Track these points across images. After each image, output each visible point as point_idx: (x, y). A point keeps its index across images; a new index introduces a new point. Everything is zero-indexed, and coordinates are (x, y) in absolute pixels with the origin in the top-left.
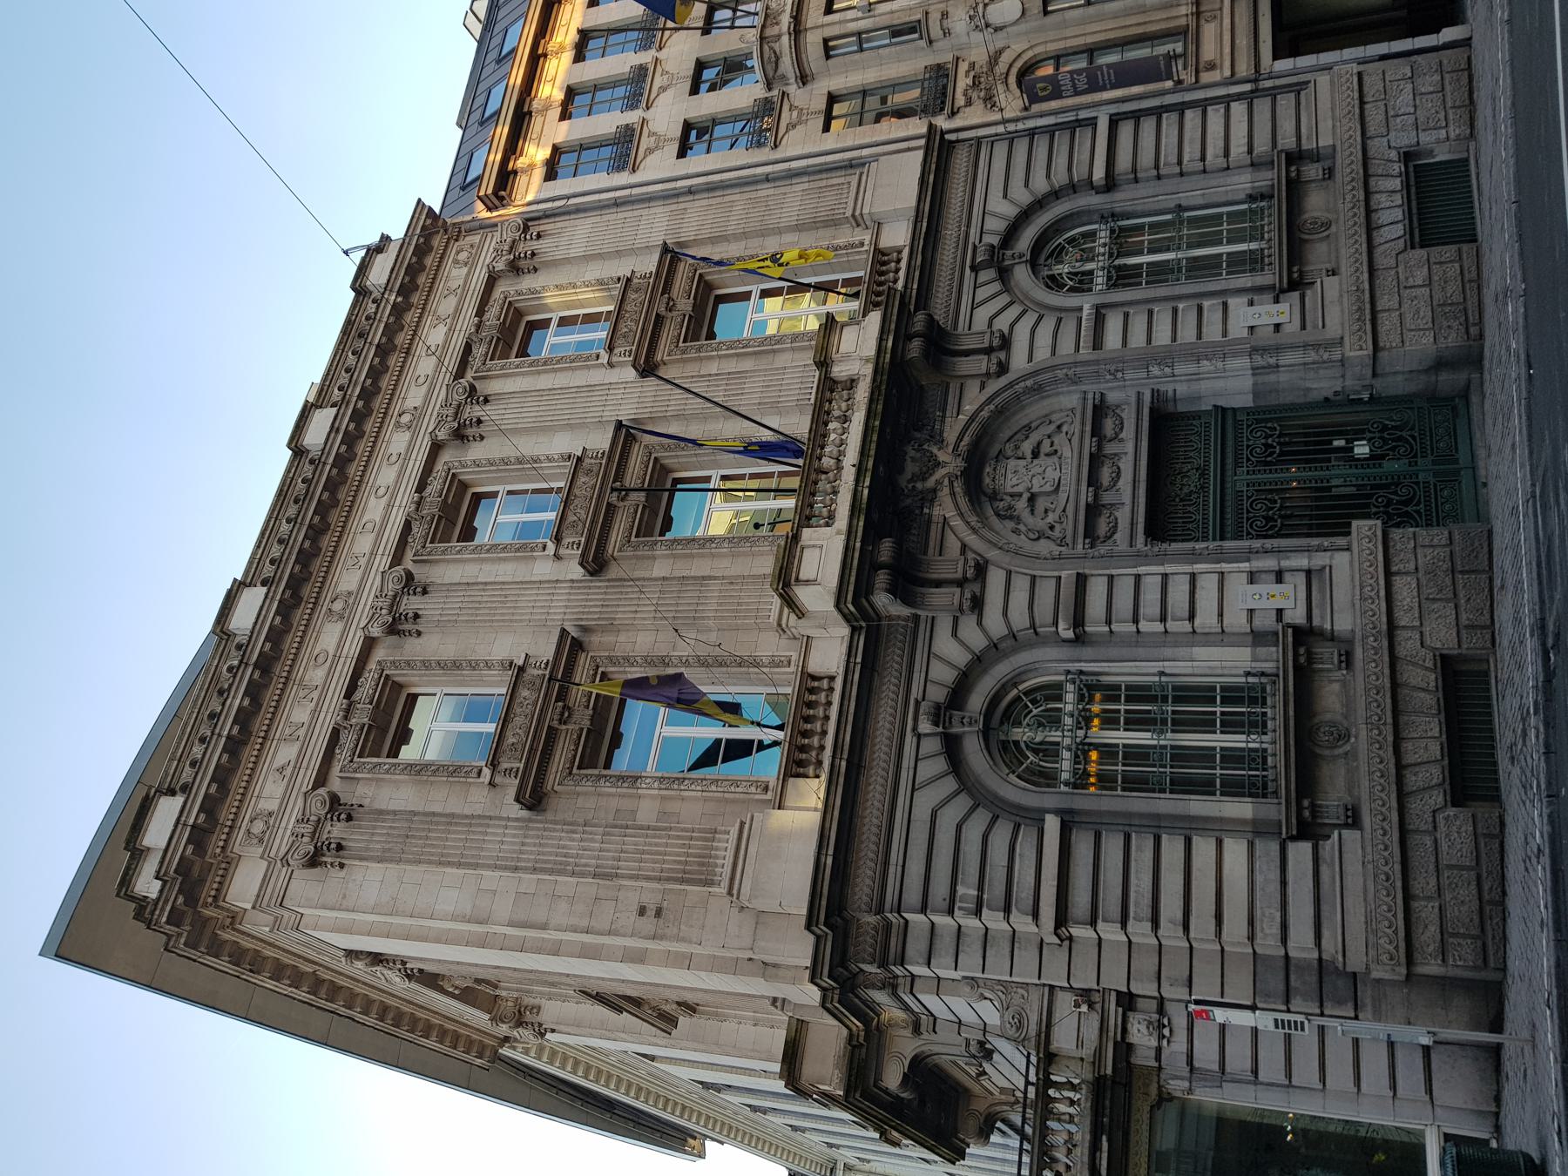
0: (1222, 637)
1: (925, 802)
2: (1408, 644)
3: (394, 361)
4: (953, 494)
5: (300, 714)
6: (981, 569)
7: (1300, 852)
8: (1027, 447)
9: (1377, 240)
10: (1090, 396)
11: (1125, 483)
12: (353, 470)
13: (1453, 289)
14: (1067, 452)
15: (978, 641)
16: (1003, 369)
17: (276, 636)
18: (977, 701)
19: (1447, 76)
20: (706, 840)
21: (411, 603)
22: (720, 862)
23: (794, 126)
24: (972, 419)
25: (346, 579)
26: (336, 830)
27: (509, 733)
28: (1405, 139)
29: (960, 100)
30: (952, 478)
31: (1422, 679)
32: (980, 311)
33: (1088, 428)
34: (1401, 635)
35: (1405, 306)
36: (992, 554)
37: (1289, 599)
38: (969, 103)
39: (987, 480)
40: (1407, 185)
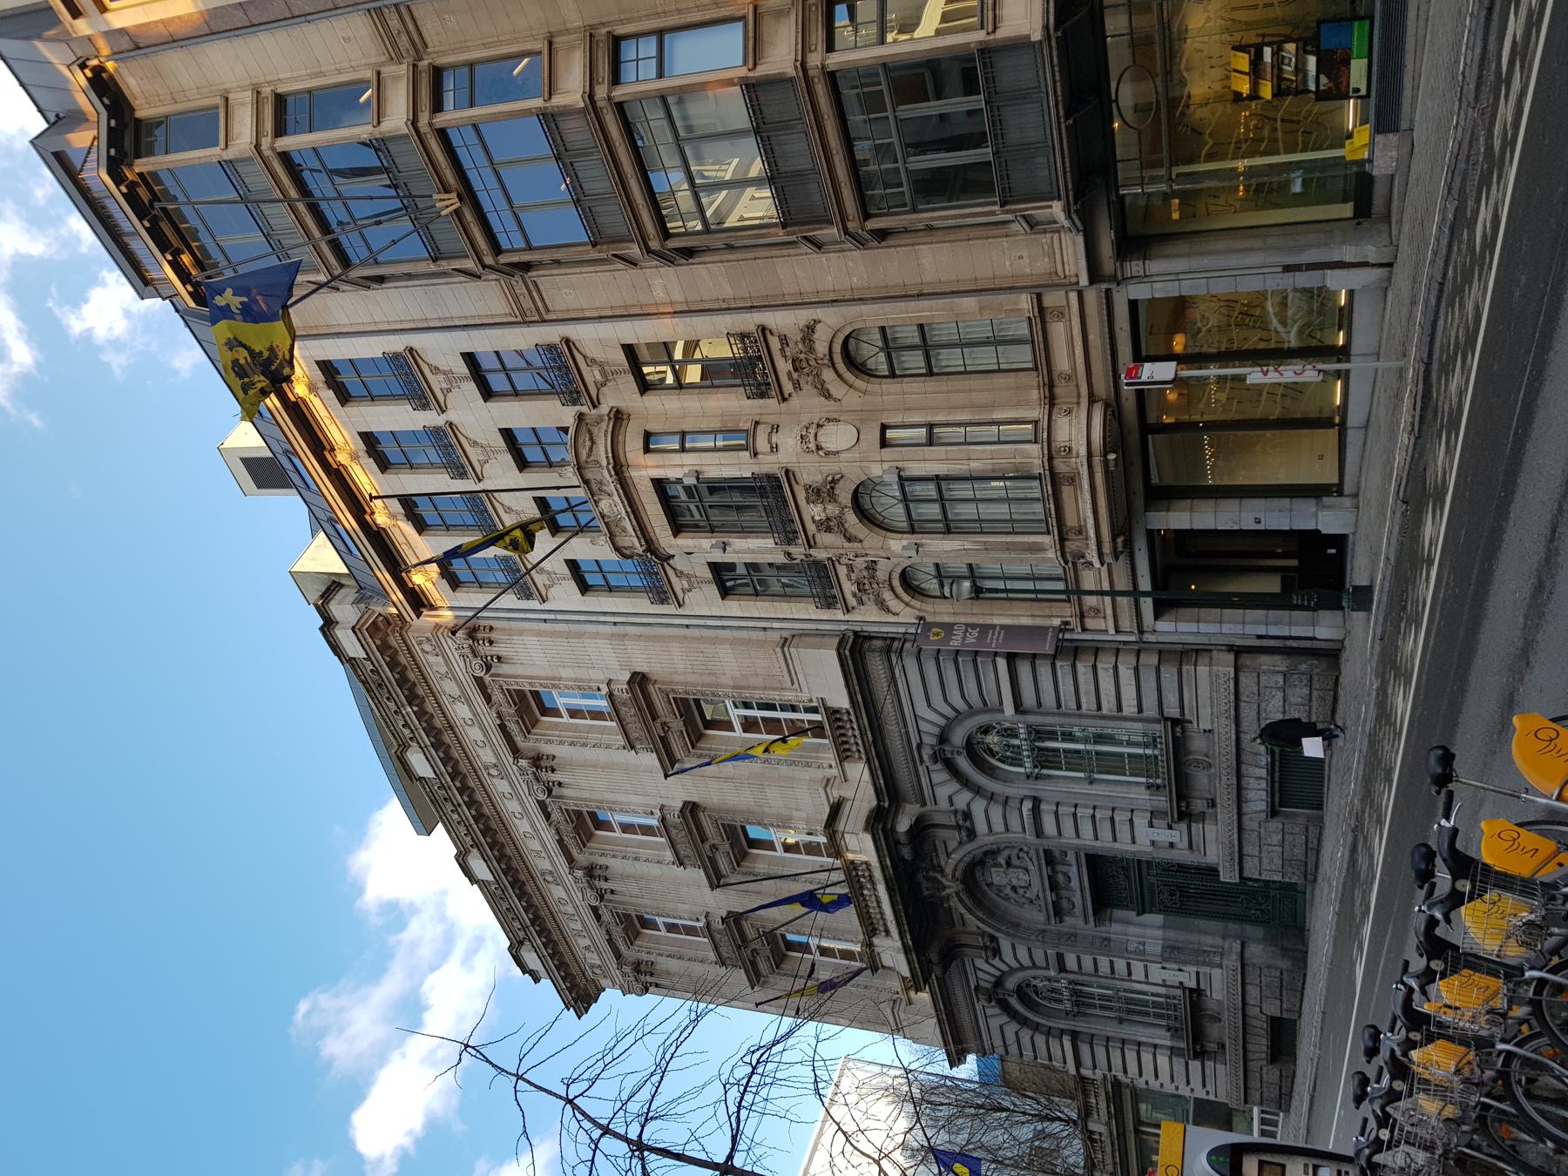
1: (994, 1023)
2: (1253, 1011)
8: (1001, 860)
11: (1075, 884)
13: (1299, 852)
14: (1031, 867)
16: (972, 834)
19: (1315, 694)
31: (1260, 1025)
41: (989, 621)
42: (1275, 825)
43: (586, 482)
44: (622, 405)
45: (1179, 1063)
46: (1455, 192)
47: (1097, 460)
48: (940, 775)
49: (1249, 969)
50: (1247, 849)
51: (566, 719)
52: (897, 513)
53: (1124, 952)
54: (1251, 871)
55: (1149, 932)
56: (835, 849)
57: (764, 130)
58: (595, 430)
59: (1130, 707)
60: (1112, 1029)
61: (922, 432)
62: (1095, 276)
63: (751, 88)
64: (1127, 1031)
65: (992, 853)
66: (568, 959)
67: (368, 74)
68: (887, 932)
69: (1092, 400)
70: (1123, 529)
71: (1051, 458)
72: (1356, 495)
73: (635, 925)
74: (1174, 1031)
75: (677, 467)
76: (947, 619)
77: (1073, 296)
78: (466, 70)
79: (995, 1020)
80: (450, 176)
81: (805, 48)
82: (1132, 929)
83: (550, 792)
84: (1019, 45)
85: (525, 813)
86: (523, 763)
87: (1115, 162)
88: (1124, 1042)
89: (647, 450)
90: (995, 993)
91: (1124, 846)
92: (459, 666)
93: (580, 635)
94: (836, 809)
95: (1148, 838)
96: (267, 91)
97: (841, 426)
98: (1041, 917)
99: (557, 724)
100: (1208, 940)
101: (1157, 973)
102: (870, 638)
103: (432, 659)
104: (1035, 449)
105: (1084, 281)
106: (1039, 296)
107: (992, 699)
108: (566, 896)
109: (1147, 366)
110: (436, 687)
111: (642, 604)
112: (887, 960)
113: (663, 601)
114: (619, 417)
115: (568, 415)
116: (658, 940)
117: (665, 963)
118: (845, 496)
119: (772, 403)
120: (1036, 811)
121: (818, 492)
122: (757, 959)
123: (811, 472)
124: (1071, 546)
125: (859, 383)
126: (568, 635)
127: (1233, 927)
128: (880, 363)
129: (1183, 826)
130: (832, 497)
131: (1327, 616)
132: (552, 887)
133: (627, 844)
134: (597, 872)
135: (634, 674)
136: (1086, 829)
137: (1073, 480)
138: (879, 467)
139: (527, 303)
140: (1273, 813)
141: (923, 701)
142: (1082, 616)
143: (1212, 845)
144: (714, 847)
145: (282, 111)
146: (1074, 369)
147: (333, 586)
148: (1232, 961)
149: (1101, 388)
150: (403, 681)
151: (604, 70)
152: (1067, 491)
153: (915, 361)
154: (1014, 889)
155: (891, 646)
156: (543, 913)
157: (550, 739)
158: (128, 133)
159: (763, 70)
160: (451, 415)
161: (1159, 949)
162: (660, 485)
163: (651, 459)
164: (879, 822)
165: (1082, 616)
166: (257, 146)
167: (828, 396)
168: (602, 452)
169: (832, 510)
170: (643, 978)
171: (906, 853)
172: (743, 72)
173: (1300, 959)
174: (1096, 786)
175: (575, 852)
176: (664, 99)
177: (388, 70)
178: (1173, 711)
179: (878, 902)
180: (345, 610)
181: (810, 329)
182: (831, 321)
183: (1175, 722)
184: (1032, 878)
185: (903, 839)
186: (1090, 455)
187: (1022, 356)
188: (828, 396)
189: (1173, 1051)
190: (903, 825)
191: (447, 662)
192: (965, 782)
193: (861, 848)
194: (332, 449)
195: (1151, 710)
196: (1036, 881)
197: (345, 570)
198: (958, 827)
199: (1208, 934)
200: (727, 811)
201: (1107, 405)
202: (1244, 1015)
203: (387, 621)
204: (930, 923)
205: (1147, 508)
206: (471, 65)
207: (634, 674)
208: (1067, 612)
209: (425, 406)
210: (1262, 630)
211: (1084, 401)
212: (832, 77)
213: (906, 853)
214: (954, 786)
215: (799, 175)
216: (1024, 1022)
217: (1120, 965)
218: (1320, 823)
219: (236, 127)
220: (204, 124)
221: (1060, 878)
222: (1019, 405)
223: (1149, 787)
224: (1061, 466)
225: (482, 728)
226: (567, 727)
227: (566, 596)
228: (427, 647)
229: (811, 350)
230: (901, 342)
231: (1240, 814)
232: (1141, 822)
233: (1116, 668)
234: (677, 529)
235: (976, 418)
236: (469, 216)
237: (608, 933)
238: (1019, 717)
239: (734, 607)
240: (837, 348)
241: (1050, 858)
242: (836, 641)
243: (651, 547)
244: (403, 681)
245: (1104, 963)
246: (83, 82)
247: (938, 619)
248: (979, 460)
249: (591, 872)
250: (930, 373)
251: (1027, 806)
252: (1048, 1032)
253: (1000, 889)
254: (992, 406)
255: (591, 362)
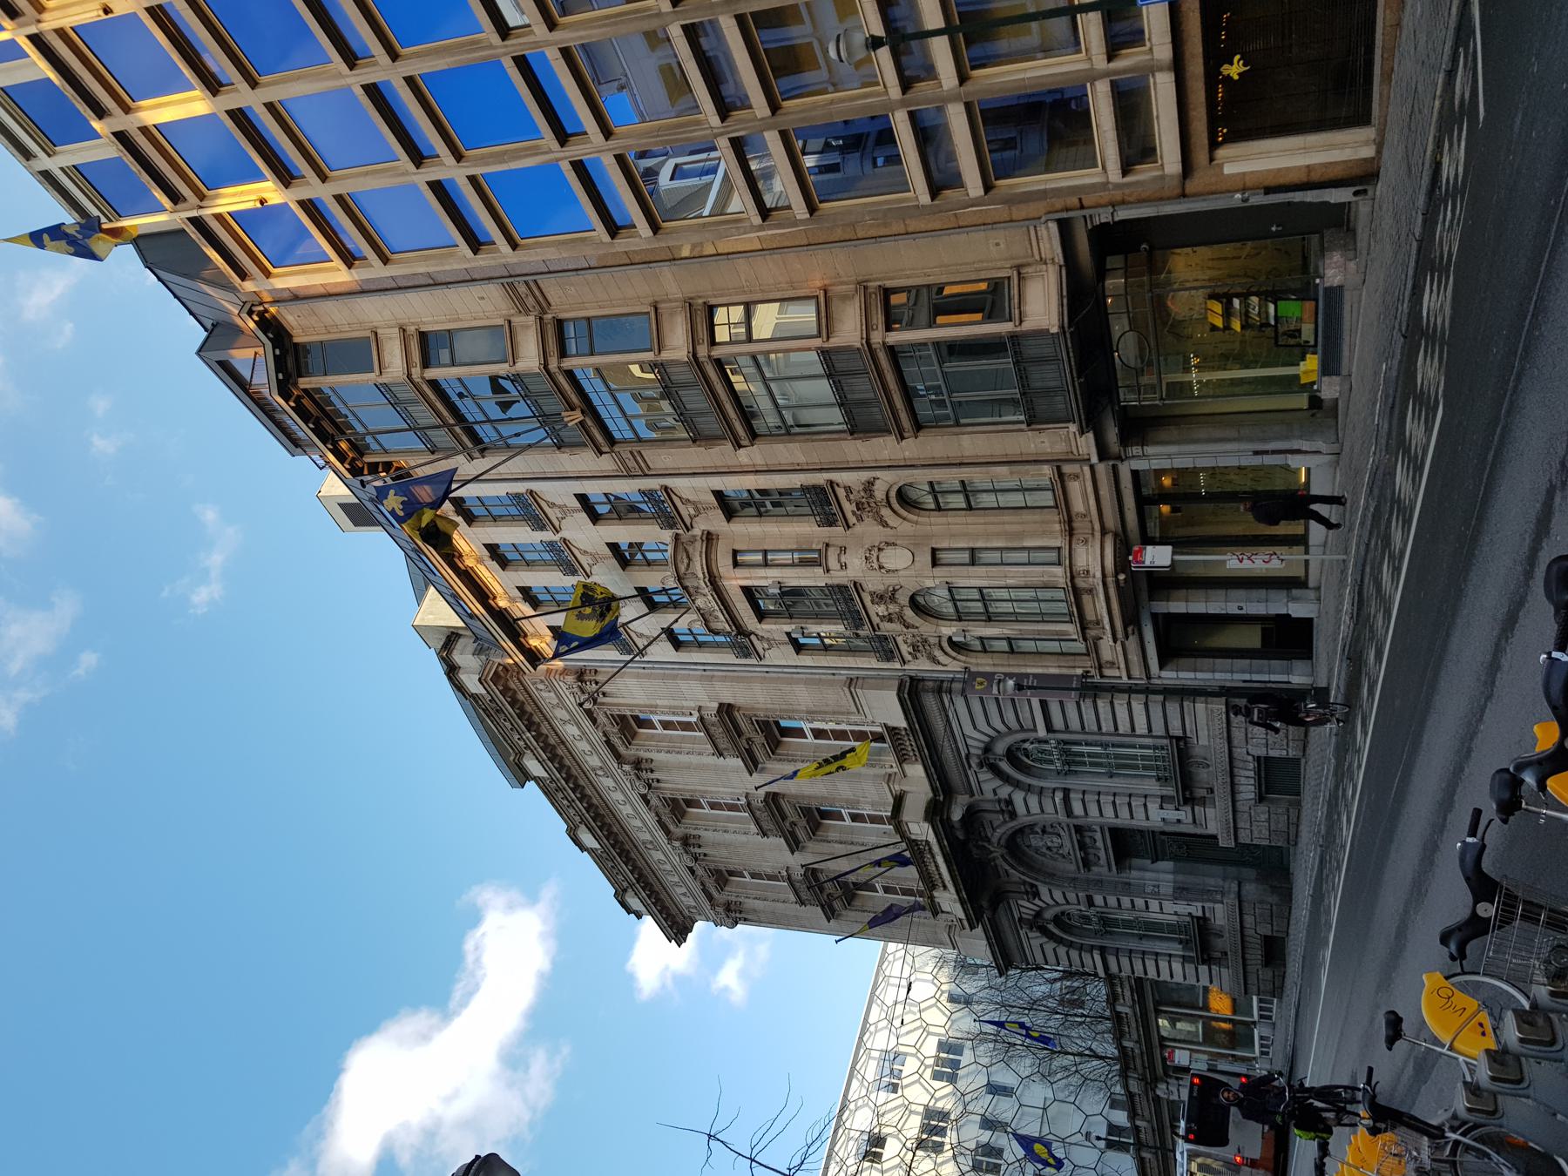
1: (1035, 943)
11: (1100, 844)
13: (1282, 826)
16: (1013, 815)
17: (610, 834)
40: (1258, 773)
41: (1023, 670)
42: (1263, 808)
43: (685, 588)
44: (712, 529)
45: (1190, 968)
46: (1376, 491)
47: (1110, 580)
48: (985, 775)
49: (1245, 904)
50: (1241, 824)
51: (660, 730)
52: (949, 609)
53: (1142, 893)
54: (1244, 838)
55: (1162, 876)
56: (900, 828)
57: (832, 373)
58: (690, 549)
59: (1141, 728)
60: (1133, 944)
61: (966, 557)
62: (1103, 454)
63: (826, 355)
64: (1147, 945)
65: (1031, 826)
66: (668, 903)
67: (500, 321)
68: (945, 887)
69: (1104, 532)
70: (1131, 620)
71: (1072, 578)
72: (1318, 588)
73: (722, 877)
74: (1185, 943)
75: (764, 578)
76: (988, 669)
77: (1087, 469)
78: (585, 323)
79: (1035, 940)
80: (574, 399)
81: (868, 327)
82: (1148, 875)
83: (650, 787)
84: (1042, 333)
85: (628, 800)
86: (627, 768)
87: (1118, 387)
88: (1144, 953)
89: (736, 564)
90: (1035, 922)
91: (1139, 821)
92: (571, 702)
93: (675, 677)
94: (899, 801)
95: (1158, 816)
96: (411, 329)
97: (899, 551)
98: (1073, 867)
99: (653, 735)
100: (1211, 881)
101: (1169, 907)
102: (923, 680)
103: (545, 694)
104: (1058, 570)
105: (1094, 459)
106: (1059, 468)
107: (1028, 724)
108: (665, 859)
109: (1149, 548)
110: (549, 714)
111: (729, 658)
112: (945, 907)
113: (747, 655)
114: (709, 538)
115: (667, 536)
116: (744, 886)
117: (750, 903)
118: (903, 599)
119: (839, 530)
120: (1066, 800)
121: (881, 597)
122: (831, 900)
123: (874, 582)
124: (1091, 633)
125: (910, 516)
126: (664, 677)
127: (1232, 870)
128: (929, 501)
129: (1188, 809)
130: (893, 599)
131: (1299, 665)
132: (653, 852)
133: (716, 819)
134: (692, 841)
135: (721, 705)
136: (1109, 811)
137: (1090, 591)
138: (933, 581)
139: (631, 464)
140: (1261, 799)
141: (970, 724)
142: (1100, 667)
143: (1213, 821)
144: (793, 824)
145: (427, 345)
146: (1088, 510)
147: (451, 639)
148: (1231, 899)
149: (1111, 521)
150: (522, 714)
151: (703, 333)
152: (1086, 599)
153: (958, 501)
154: (1049, 848)
155: (941, 688)
156: (646, 871)
157: (649, 746)
158: (290, 357)
159: (835, 342)
160: (564, 534)
161: (1170, 891)
162: (748, 592)
163: (740, 572)
164: (935, 812)
165: (1100, 667)
166: (409, 376)
167: (885, 525)
168: (698, 566)
169: (893, 608)
170: (732, 914)
171: (960, 835)
172: (818, 342)
173: (1286, 895)
174: (1115, 779)
175: (672, 827)
176: (754, 358)
177: (518, 320)
178: (1179, 733)
179: (937, 867)
180: (464, 657)
181: (870, 484)
182: (886, 481)
183: (1178, 739)
184: (1067, 843)
185: (957, 826)
186: (1104, 576)
187: (1047, 498)
188: (885, 525)
189: (1185, 959)
190: (957, 815)
191: (559, 697)
192: (1006, 779)
193: (921, 830)
194: (461, 556)
195: (1158, 729)
196: (1067, 844)
197: (461, 624)
198: (1002, 811)
199: (1212, 877)
200: (803, 797)
201: (1116, 535)
202: (1243, 935)
203: (506, 668)
204: (978, 872)
205: (1151, 599)
206: (588, 319)
207: (721, 705)
208: (1088, 663)
209: (542, 528)
210: (1247, 677)
211: (1098, 535)
212: (892, 351)
213: (960, 835)
214: (998, 782)
215: (864, 403)
216: (1060, 941)
217: (1140, 902)
218: (1299, 803)
219: (387, 358)
220: (357, 353)
221: (1088, 840)
222: (1044, 534)
223: (1159, 779)
224: (1080, 583)
225: (590, 742)
226: (661, 739)
227: (663, 651)
228: (541, 686)
229: (872, 496)
230: (945, 487)
231: (1234, 802)
232: (1153, 807)
233: (1129, 704)
234: (761, 615)
235: (1010, 545)
236: (589, 422)
237: (702, 884)
238: (1051, 735)
239: (806, 660)
240: (893, 494)
241: (1079, 829)
242: (896, 683)
243: (741, 631)
244: (522, 714)
245: (1126, 902)
246: (252, 325)
247: (981, 669)
248: (1015, 576)
249: (686, 841)
250: (970, 508)
251: (1059, 796)
252: (1081, 948)
253: (1037, 850)
254: (1020, 535)
255: (686, 502)
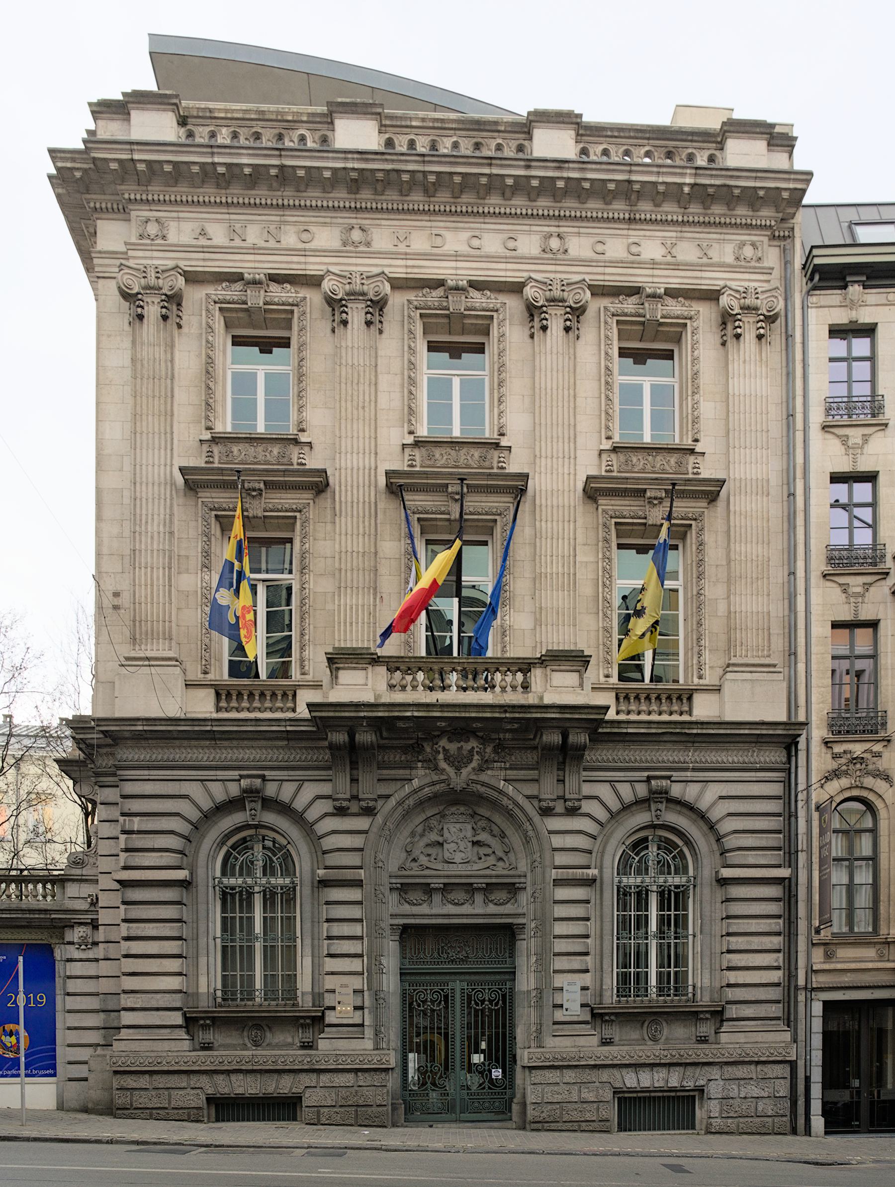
0: (317, 973)
2: (308, 1079)
3: (619, 207)
4: (433, 784)
5: (254, 235)
6: (369, 812)
7: (177, 1018)
9: (624, 1071)
10: (523, 880)
12: (494, 201)
15: (312, 815)
18: (270, 818)
19: (770, 1120)
20: (164, 633)
21: (356, 314)
22: (149, 647)
23: (845, 591)
24: (501, 792)
25: (383, 235)
26: (153, 310)
27: (241, 446)
28: (715, 1089)
29: (838, 749)
30: (447, 781)
31: (285, 1086)
32: (603, 791)
33: (494, 880)
34: (314, 1076)
35: (564, 1086)
36: (379, 819)
37: (343, 1011)
38: (835, 756)
39: (453, 809)
42: (608, 1095)
